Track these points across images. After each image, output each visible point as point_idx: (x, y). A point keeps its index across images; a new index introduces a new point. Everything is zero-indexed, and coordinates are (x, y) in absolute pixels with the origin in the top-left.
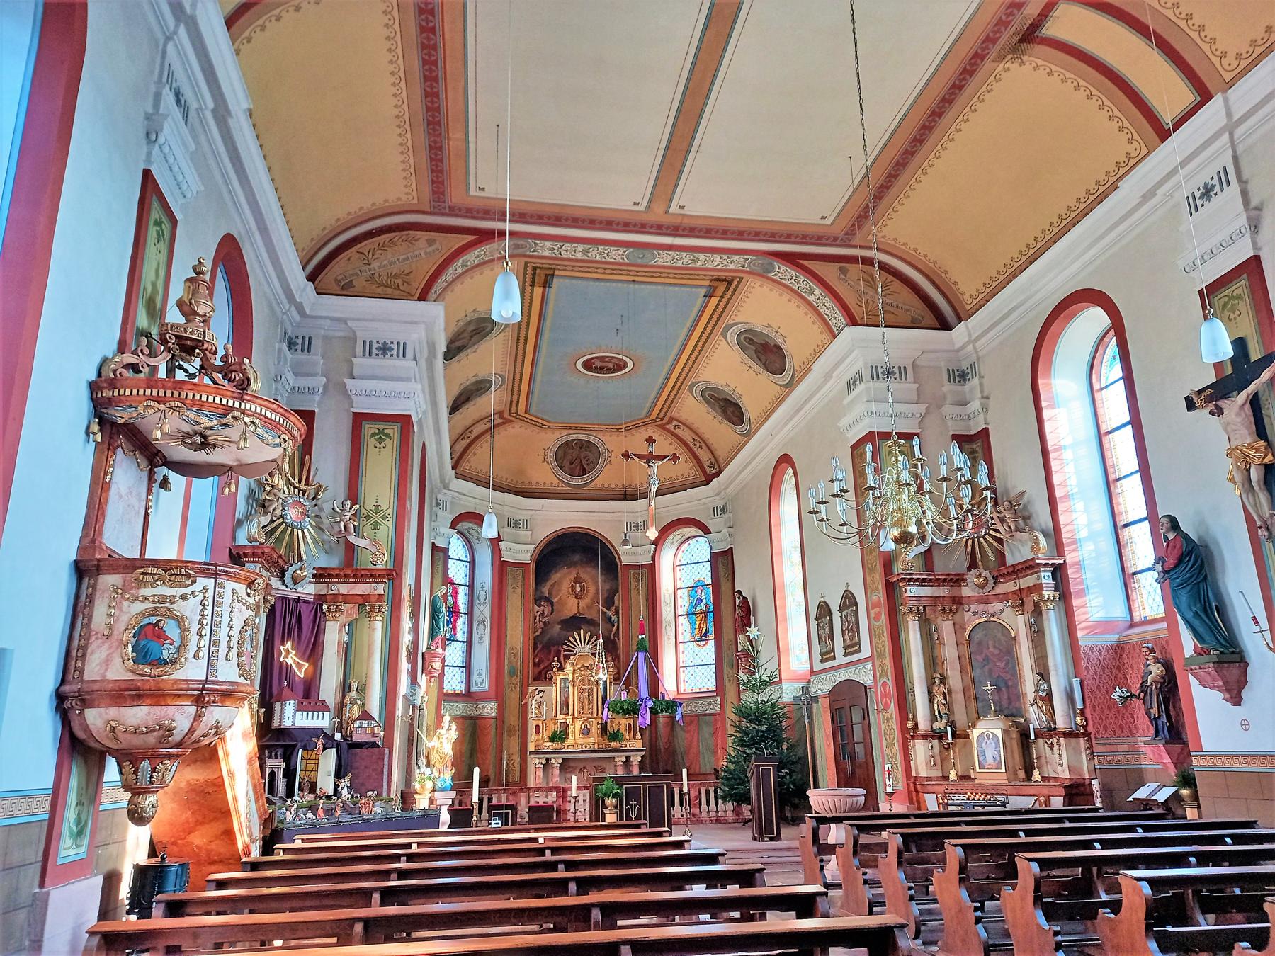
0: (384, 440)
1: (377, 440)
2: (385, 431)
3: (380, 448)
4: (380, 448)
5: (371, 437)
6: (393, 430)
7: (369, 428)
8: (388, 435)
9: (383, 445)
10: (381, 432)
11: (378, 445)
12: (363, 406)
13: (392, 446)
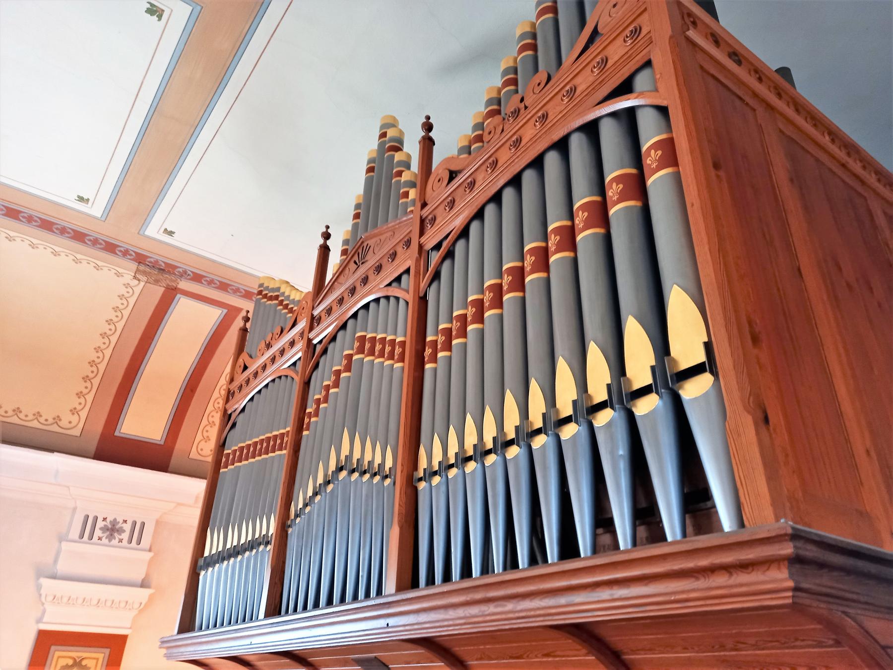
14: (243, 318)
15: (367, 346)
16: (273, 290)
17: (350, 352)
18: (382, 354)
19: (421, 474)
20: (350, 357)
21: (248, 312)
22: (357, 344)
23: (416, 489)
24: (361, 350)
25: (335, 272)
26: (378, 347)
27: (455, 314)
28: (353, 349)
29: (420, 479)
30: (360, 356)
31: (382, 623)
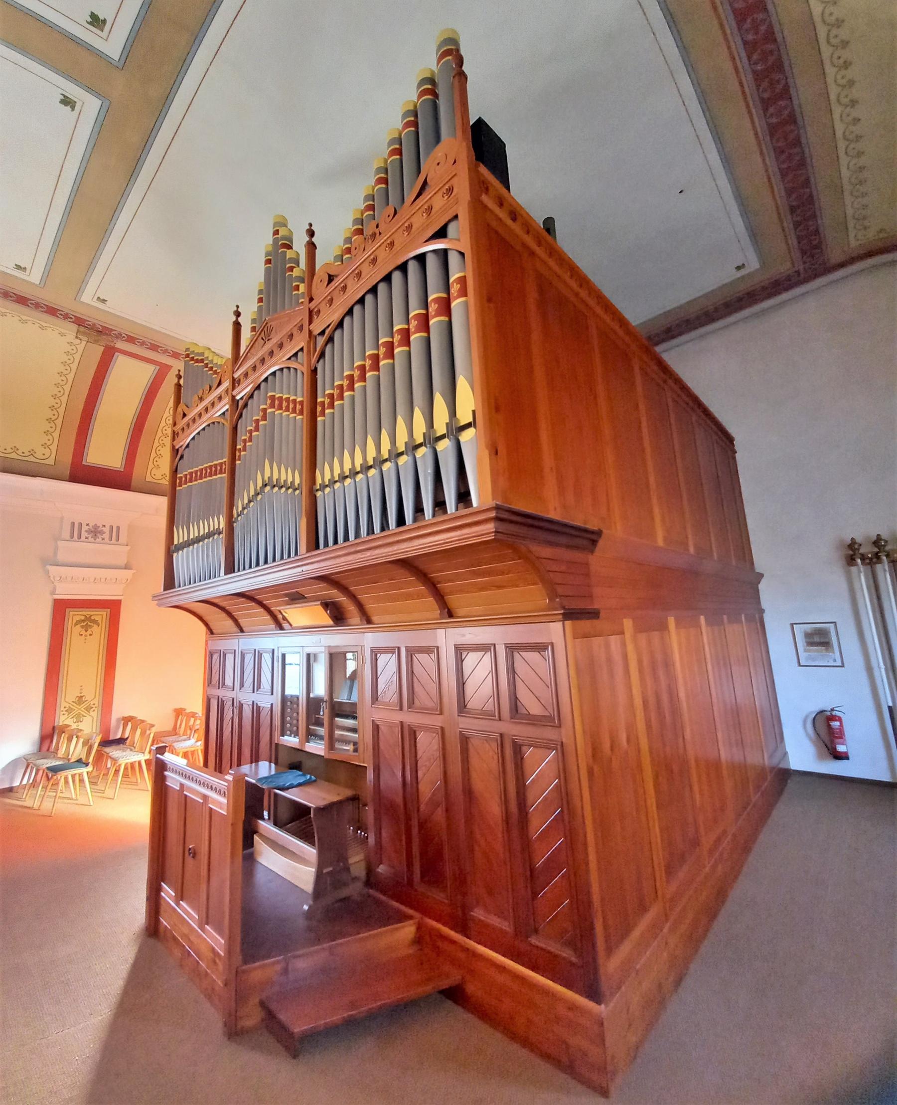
0: (91, 627)
1: (82, 627)
2: (92, 618)
3: (86, 636)
4: (86, 636)
5: (76, 624)
6: (101, 615)
7: (74, 616)
8: (95, 622)
9: (89, 632)
10: (88, 619)
11: (83, 632)
12: (66, 592)
13: (99, 633)
14: (177, 375)
15: (277, 402)
16: (198, 354)
17: (265, 407)
18: (287, 409)
19: (318, 487)
20: (265, 410)
21: (179, 371)
22: (269, 402)
23: (315, 496)
24: (272, 406)
25: (248, 344)
26: (284, 404)
28: (266, 405)
29: (317, 490)
30: (273, 410)
31: (299, 569)
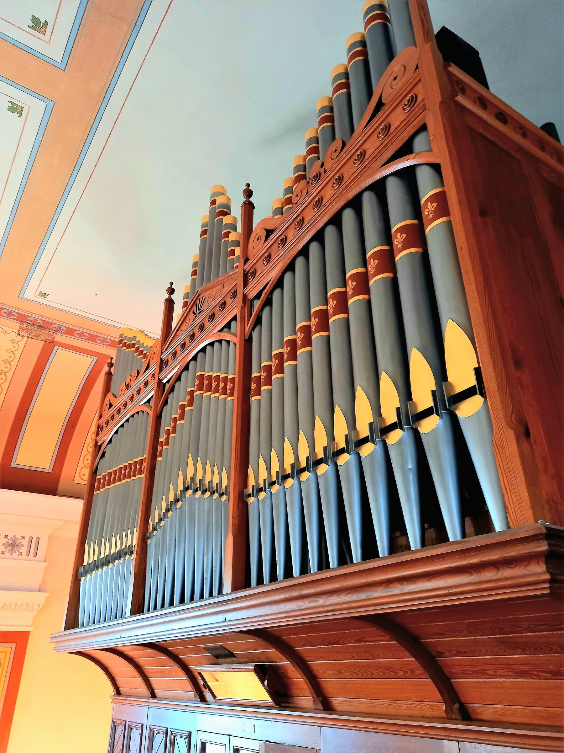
27: (274, 353)
